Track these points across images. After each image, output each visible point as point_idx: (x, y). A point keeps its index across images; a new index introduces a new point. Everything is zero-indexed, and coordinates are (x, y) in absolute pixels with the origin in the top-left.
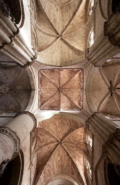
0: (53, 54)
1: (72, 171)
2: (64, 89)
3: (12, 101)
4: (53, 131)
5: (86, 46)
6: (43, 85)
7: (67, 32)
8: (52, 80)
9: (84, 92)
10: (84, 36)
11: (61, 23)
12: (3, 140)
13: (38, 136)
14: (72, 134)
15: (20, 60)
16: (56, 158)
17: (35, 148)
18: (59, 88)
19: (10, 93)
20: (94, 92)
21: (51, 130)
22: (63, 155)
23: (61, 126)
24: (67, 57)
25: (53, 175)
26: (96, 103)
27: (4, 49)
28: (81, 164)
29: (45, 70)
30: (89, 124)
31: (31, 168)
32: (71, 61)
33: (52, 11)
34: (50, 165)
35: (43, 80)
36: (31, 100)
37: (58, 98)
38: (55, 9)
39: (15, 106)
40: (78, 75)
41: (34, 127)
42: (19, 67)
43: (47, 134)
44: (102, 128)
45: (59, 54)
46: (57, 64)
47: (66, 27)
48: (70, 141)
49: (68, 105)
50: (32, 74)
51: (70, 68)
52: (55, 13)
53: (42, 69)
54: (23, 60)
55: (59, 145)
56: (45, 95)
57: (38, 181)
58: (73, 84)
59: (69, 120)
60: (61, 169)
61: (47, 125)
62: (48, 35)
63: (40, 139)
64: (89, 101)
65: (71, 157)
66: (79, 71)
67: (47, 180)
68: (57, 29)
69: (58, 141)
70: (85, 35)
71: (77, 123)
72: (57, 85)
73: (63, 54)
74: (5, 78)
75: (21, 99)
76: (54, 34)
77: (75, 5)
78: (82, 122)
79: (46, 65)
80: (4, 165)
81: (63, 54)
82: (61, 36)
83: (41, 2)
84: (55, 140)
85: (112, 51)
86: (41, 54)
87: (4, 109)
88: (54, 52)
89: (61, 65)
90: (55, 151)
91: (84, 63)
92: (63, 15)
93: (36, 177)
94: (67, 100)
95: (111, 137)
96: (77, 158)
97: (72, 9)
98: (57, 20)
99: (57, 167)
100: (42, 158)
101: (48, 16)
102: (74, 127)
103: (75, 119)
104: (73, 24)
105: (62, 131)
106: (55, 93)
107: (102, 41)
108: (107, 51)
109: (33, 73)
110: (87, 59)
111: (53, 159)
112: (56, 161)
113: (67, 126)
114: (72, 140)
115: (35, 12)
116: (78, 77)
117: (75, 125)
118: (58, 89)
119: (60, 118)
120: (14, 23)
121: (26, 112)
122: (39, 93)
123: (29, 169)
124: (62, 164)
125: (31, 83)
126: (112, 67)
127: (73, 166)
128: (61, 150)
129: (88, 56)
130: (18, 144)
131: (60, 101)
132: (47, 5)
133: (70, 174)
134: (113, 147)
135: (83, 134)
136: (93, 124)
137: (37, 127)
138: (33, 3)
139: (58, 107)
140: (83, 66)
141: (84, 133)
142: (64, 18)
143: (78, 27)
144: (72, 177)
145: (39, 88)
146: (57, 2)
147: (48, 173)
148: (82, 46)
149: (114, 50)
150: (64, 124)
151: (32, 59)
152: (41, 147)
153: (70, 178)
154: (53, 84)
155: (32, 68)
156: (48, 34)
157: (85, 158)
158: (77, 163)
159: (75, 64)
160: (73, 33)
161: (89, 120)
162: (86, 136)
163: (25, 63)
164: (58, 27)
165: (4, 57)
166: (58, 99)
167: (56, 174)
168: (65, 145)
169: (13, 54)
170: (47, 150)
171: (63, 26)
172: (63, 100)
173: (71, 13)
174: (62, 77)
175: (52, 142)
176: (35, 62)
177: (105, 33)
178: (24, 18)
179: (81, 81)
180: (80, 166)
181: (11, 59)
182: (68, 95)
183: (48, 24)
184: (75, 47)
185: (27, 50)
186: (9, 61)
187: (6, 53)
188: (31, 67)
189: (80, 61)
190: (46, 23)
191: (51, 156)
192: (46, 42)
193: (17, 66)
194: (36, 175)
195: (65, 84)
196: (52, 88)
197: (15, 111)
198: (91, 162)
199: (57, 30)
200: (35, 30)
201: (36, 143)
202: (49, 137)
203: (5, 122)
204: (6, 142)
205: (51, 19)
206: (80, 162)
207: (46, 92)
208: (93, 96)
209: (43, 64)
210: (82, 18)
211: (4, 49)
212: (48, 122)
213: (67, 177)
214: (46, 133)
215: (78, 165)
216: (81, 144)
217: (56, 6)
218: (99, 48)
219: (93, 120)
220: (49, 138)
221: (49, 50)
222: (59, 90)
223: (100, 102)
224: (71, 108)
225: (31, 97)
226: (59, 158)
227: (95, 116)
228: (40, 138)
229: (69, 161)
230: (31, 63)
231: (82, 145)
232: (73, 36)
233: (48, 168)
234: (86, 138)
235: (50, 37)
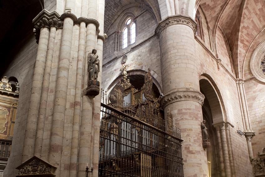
16: (254, 9)
25: (258, 36)
57: (237, 58)
80: (204, 129)
93: (232, 54)
99: (260, 21)
100: (227, 23)
111: (247, 14)
147: (247, 38)
167: (262, 31)
194: (231, 51)
201: (206, 18)
228: (207, 4)
233: (245, 31)
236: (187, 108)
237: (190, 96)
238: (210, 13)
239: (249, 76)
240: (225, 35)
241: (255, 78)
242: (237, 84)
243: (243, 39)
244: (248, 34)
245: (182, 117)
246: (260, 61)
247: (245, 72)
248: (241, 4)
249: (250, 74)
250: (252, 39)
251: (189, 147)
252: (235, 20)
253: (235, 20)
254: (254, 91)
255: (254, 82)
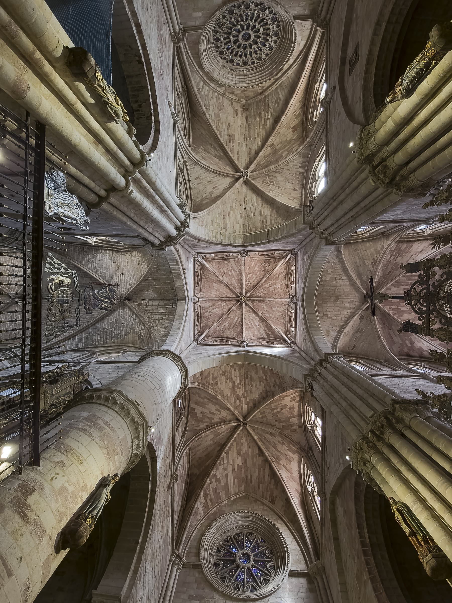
0: (227, 218)
1: (272, 494)
2: (250, 297)
3: (134, 326)
4: (225, 395)
5: (305, 197)
6: (203, 290)
7: (259, 165)
8: (224, 276)
9: (299, 304)
10: (300, 173)
11: (244, 145)
12: (106, 423)
13: (193, 405)
14: (271, 403)
15: (151, 230)
16: (233, 461)
17: (184, 434)
18: (239, 295)
19: (129, 308)
20: (324, 305)
21: (222, 393)
22: (250, 454)
23: (245, 384)
24: (259, 224)
26: (328, 332)
27: (109, 203)
28: (292, 477)
29: (208, 255)
30: (313, 382)
31: (173, 486)
32: (268, 234)
33: (224, 115)
34: (218, 476)
35: (203, 277)
36: (176, 323)
37: (237, 318)
38: (231, 110)
39: (139, 337)
40: (284, 266)
41: (181, 388)
42: (149, 249)
43: (212, 401)
44: (350, 395)
45: (241, 217)
46: (234, 240)
47: (257, 153)
48: (265, 419)
49: (259, 336)
50: (178, 264)
51: (265, 249)
52: (231, 120)
53: (201, 253)
54: (157, 231)
55: (240, 430)
56: (206, 312)
57: (191, 515)
58: (271, 286)
59: (264, 370)
60: (245, 487)
61: (211, 382)
62: (213, 172)
63: (196, 414)
64: (310, 327)
65: (270, 459)
66: (287, 255)
67: (212, 514)
68: (235, 158)
69: (238, 419)
70: (301, 170)
71: (283, 377)
72: (235, 288)
73: (248, 216)
74: (118, 273)
75: (154, 321)
76: (229, 170)
77: (278, 99)
78: (294, 376)
79: (210, 243)
81: (248, 216)
82: (245, 174)
83: (198, 96)
84: (229, 417)
85: (376, 203)
86: (198, 218)
87: (114, 343)
88: (229, 213)
89: (244, 243)
90: (229, 444)
91: (299, 237)
92: (249, 125)
93: (185, 507)
94: (257, 323)
95: (378, 423)
96: (283, 462)
97: (271, 110)
98: (236, 138)
100: (200, 458)
101: (214, 127)
102: (275, 387)
103: (278, 370)
104: (273, 144)
105: (248, 395)
106: (230, 306)
107: (350, 179)
108: (362, 205)
109: (181, 261)
110: (308, 226)
112: (233, 467)
113: (258, 383)
114: (270, 417)
115: (184, 120)
116: (283, 270)
117: (278, 383)
118: (239, 297)
119: (243, 365)
120: (134, 141)
121: (164, 351)
122: (194, 306)
123: (169, 487)
124: (247, 477)
125: (177, 284)
126: (368, 244)
127: (273, 481)
128: (243, 440)
129: (310, 218)
130: (142, 433)
131: (241, 324)
132: (211, 102)
133: (267, 502)
134: (386, 451)
135: (296, 405)
136: (325, 384)
137: (189, 386)
138: (179, 98)
139: (238, 338)
140: (297, 245)
141: (300, 401)
142: (252, 131)
143: (287, 152)
144: (271, 509)
145: (194, 296)
146: (236, 95)
148: (296, 196)
149: (382, 199)
150: (252, 379)
151: (177, 228)
152: (197, 433)
153: (266, 513)
154: (227, 286)
155: (177, 251)
156: (215, 172)
157: (304, 465)
158: (283, 474)
159: (277, 240)
160: (272, 167)
161: (313, 373)
162: (304, 409)
163: (162, 239)
164: (238, 154)
165: (114, 224)
166: (237, 321)
167: (232, 499)
168: (254, 430)
169: (132, 215)
170: (211, 440)
171: (250, 151)
172: (247, 321)
173: (268, 119)
174: (247, 271)
175: (223, 421)
176: (186, 236)
177: (362, 156)
178: (157, 130)
179: (290, 278)
180: (291, 483)
181: (130, 228)
182: (260, 312)
183: (214, 148)
184: (277, 199)
185: (165, 207)
186: (125, 233)
187: (115, 213)
188: (175, 248)
189: (291, 232)
190: (208, 146)
191: (222, 456)
192: (209, 189)
193: (144, 246)
194: (186, 501)
195: (254, 287)
196: (224, 296)
197: (140, 348)
198: (319, 476)
199: (236, 162)
200: (185, 162)
201: (187, 423)
202: (215, 410)
203: (115, 375)
204: (112, 429)
205: (221, 136)
206: (292, 473)
207: (210, 304)
208: (321, 315)
209: (203, 241)
210: (294, 129)
211: (109, 203)
212: (215, 375)
213: (259, 510)
214: (209, 399)
215: (285, 480)
216: (293, 428)
217: (234, 103)
218: (341, 198)
219: (324, 372)
220: (217, 412)
221: (216, 208)
222: (238, 301)
223: (338, 329)
224: (267, 342)
225: (176, 316)
226: (239, 461)
227: (329, 363)
229: (264, 469)
230: (176, 238)
231: (295, 430)
232: (272, 174)
233: (214, 485)
234: (304, 416)
235: (220, 178)
236: (111, 423)
237: (131, 413)
238: (193, 423)
239: (193, 560)
240: (190, 474)
241: (201, 568)
242: (171, 561)
243: (208, 493)
244: (216, 489)
245: (87, 428)
246: (216, 545)
247: (190, 548)
248: (224, 444)
249: (196, 556)
250: (217, 503)
251: (32, 492)
252: (210, 461)
253: (210, 461)
254: (190, 596)
255: (197, 575)
